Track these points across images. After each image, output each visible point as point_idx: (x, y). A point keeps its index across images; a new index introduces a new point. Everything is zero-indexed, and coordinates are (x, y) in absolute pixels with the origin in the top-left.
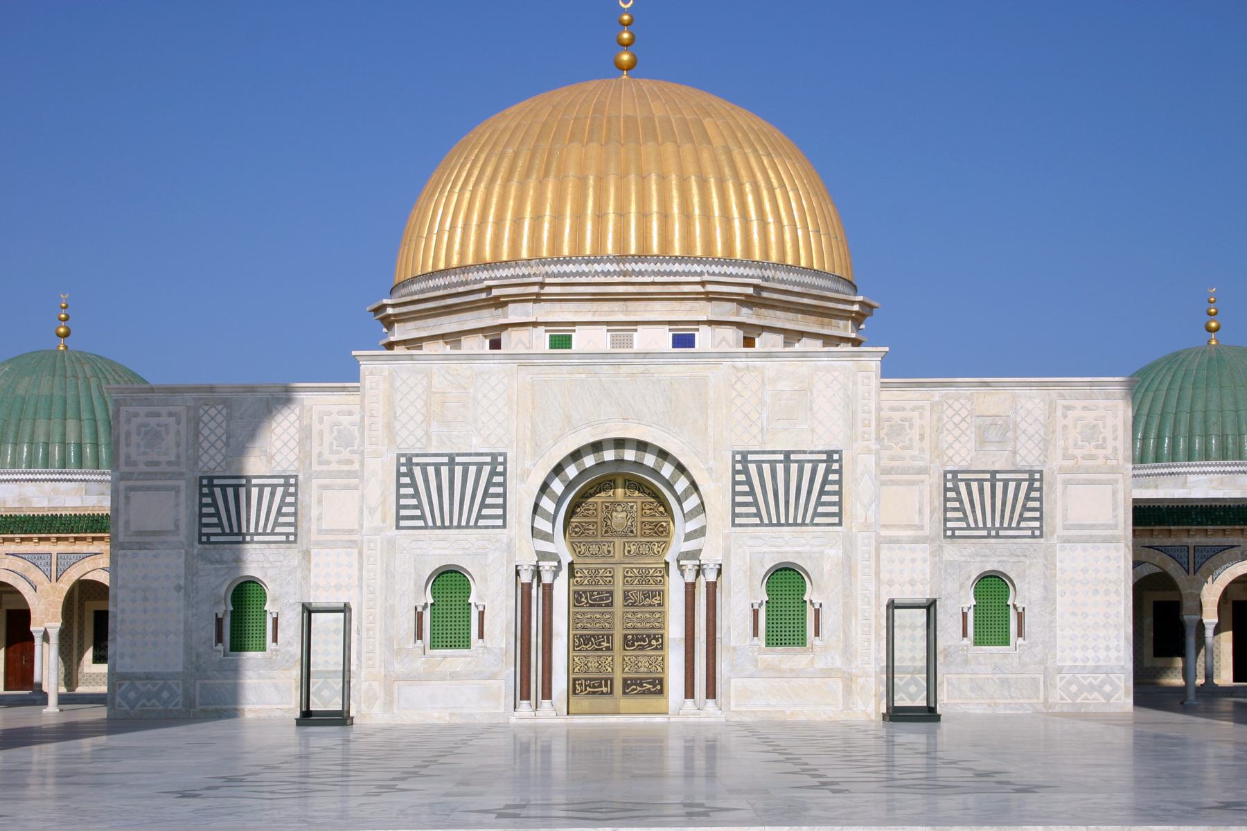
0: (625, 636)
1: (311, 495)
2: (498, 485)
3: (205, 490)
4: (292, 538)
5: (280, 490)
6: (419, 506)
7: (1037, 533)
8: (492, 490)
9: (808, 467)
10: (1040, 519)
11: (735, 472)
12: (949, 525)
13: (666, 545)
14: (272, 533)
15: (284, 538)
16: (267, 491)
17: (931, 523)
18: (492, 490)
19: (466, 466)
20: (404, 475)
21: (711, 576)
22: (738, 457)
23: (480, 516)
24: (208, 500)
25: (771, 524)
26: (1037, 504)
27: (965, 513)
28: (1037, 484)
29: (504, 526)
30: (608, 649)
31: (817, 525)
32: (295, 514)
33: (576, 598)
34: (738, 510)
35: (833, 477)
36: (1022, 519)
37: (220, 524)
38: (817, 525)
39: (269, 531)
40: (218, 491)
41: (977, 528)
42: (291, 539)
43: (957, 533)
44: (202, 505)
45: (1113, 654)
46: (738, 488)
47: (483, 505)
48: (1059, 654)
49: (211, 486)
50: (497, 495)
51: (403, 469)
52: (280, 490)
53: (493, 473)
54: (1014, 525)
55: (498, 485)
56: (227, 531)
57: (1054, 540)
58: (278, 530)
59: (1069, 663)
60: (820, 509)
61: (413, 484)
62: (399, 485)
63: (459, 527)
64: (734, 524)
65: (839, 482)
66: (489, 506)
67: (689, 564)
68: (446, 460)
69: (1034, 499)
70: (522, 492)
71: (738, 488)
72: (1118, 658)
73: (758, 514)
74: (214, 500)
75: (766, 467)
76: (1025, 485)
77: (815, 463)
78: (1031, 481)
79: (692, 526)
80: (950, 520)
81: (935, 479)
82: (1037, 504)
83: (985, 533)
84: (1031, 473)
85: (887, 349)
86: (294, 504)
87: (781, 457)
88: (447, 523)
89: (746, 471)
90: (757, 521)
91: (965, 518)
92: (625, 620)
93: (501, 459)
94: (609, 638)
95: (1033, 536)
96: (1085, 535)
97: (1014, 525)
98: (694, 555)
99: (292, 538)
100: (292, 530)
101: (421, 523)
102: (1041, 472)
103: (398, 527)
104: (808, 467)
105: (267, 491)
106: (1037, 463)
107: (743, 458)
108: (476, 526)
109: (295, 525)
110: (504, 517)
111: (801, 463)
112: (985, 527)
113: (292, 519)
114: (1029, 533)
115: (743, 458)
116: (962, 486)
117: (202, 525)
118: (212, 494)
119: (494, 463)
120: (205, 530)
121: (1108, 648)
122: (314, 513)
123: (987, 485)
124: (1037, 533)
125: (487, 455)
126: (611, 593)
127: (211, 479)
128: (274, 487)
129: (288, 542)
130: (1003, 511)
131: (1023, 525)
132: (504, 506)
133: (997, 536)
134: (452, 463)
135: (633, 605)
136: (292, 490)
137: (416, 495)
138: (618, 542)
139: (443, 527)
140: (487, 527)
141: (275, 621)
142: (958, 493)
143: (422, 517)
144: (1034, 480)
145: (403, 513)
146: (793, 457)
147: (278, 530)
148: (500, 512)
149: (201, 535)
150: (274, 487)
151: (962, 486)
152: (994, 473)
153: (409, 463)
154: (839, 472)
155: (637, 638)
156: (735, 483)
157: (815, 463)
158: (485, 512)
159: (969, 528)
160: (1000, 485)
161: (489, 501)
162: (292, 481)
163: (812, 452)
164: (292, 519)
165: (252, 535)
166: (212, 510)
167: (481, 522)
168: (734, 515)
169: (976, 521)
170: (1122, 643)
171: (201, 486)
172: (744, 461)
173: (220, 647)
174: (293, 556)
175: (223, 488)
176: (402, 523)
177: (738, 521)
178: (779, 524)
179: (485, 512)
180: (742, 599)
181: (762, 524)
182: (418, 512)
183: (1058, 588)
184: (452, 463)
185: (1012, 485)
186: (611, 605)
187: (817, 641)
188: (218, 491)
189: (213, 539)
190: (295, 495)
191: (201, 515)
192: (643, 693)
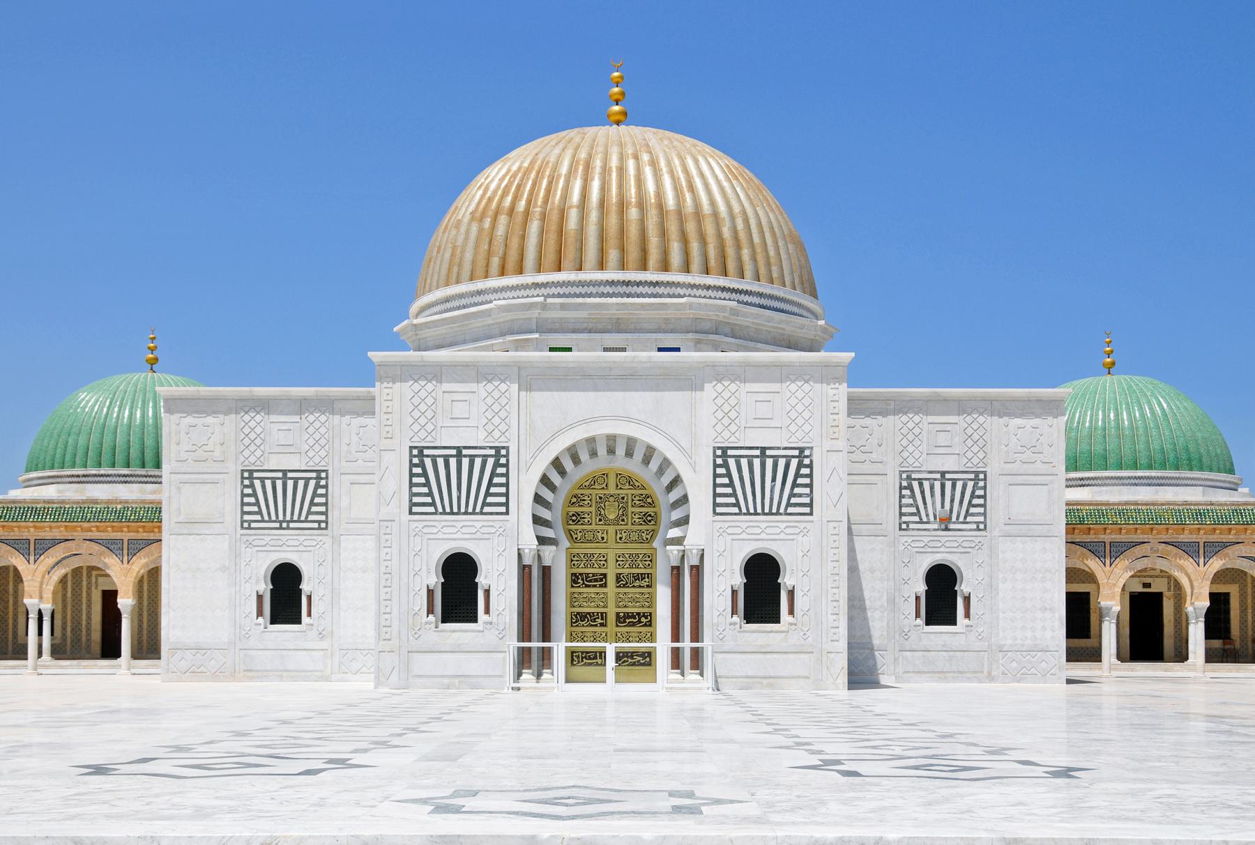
0: (618, 614)
1: (338, 488)
2: (502, 475)
3: (247, 482)
4: (323, 525)
5: (312, 483)
6: (430, 494)
7: (982, 526)
8: (496, 480)
9: (782, 462)
10: (985, 514)
11: (716, 466)
12: (904, 519)
13: (654, 533)
14: (306, 521)
15: (316, 525)
16: (301, 484)
17: (890, 516)
18: (496, 480)
19: (472, 459)
20: (416, 465)
21: (695, 562)
22: (719, 452)
23: (484, 504)
24: (249, 491)
25: (748, 513)
26: (981, 501)
27: (918, 509)
28: (981, 484)
29: (507, 513)
30: (602, 625)
31: (790, 514)
32: (326, 504)
33: (575, 579)
34: (719, 500)
35: (805, 471)
37: (260, 513)
38: (790, 514)
39: (303, 518)
40: (257, 483)
42: (323, 526)
44: (243, 495)
45: (1048, 634)
46: (719, 481)
47: (488, 494)
48: (1001, 634)
49: (251, 478)
50: (501, 485)
51: (416, 461)
52: (312, 483)
53: (497, 465)
54: (961, 519)
55: (502, 475)
56: (266, 518)
57: (996, 533)
58: (311, 518)
59: (1009, 642)
60: (793, 500)
61: (425, 474)
62: (412, 475)
63: (466, 513)
64: (715, 513)
65: (810, 476)
66: (494, 496)
67: (674, 550)
68: (454, 452)
69: (979, 497)
70: (524, 485)
71: (719, 481)
72: (1052, 637)
73: (737, 505)
74: (254, 491)
75: (744, 462)
76: (970, 484)
77: (789, 459)
78: (976, 479)
79: (676, 515)
80: (905, 514)
81: (893, 481)
82: (981, 501)
84: (977, 473)
85: (853, 354)
86: (326, 495)
87: (757, 452)
88: (455, 510)
89: (725, 465)
90: (736, 510)
92: (618, 599)
93: (503, 452)
94: (603, 616)
95: (978, 529)
96: (1023, 529)
97: (961, 519)
98: (678, 541)
99: (323, 525)
100: (323, 518)
101: (432, 509)
102: (985, 473)
103: (411, 513)
104: (782, 462)
105: (301, 484)
106: (981, 464)
107: (723, 453)
108: (482, 513)
109: (325, 513)
110: (506, 504)
111: (776, 458)
113: (323, 509)
114: (974, 526)
115: (723, 453)
116: (915, 485)
117: (243, 513)
118: (252, 486)
119: (498, 456)
120: (246, 517)
121: (1044, 628)
122: (344, 503)
124: (982, 526)
125: (491, 448)
126: (605, 575)
127: (251, 472)
128: (307, 480)
129: (320, 528)
132: (507, 495)
134: (459, 456)
135: (624, 586)
136: (323, 482)
137: (427, 484)
138: (611, 529)
139: (452, 513)
140: (491, 514)
141: (309, 598)
142: (912, 491)
143: (433, 504)
144: (979, 477)
145: (416, 500)
146: (768, 452)
147: (311, 518)
148: (503, 500)
149: (243, 521)
150: (307, 480)
152: (943, 474)
153: (421, 455)
154: (810, 466)
155: (627, 616)
156: (716, 476)
157: (789, 459)
158: (490, 500)
159: (921, 522)
160: (948, 485)
161: (493, 490)
162: (323, 475)
163: (786, 448)
164: (323, 509)
165: (288, 522)
166: (252, 500)
167: (486, 509)
168: (715, 505)
170: (1057, 624)
171: (243, 478)
172: (724, 455)
173: (260, 619)
174: (324, 539)
175: (262, 480)
176: (415, 509)
177: (719, 510)
178: (756, 514)
179: (490, 500)
180: (724, 581)
181: (740, 514)
182: (429, 500)
183: (1001, 576)
184: (459, 456)
185: (959, 485)
186: (605, 585)
187: (790, 619)
188: (257, 483)
189: (253, 525)
190: (326, 487)
191: (243, 504)
192: (634, 664)
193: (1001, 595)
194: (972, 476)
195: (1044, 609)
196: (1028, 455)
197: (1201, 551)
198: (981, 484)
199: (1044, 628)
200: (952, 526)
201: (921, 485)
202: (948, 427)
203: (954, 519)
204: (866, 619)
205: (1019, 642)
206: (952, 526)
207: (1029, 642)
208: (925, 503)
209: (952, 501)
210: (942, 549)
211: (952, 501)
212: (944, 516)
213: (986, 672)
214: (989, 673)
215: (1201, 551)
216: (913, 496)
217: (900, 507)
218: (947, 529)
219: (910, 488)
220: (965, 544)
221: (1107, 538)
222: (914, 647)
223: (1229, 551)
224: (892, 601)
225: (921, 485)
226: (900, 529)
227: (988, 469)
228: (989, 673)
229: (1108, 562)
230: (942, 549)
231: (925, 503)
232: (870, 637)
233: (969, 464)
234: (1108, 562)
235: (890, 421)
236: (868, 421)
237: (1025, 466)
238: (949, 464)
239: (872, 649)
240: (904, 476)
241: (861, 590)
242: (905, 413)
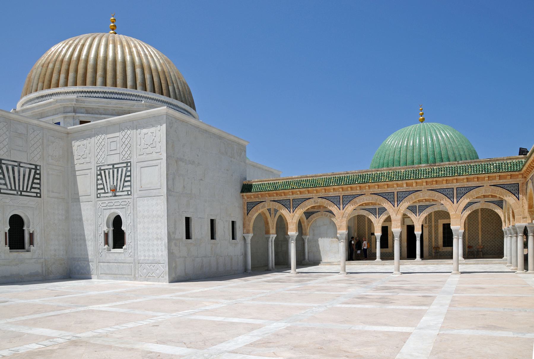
7: (129, 193)
28: (129, 169)
36: (124, 186)
41: (107, 193)
43: (102, 195)
45: (160, 253)
48: (139, 253)
59: (143, 258)
69: (128, 176)
72: (162, 255)
76: (125, 169)
81: (94, 172)
83: (15, 192)
84: (127, 163)
91: (103, 189)
96: (148, 193)
112: (15, 190)
114: (126, 193)
116: (103, 172)
123: (111, 171)
130: (19, 180)
131: (125, 189)
133: (21, 195)
142: (102, 176)
151: (103, 172)
152: (113, 165)
159: (105, 193)
160: (116, 170)
163: (9, 160)
169: (11, 186)
170: (163, 247)
185: (120, 170)
193: (138, 231)
194: (125, 165)
195: (158, 239)
196: (150, 150)
197: (341, 201)
198: (129, 169)
199: (158, 250)
200: (117, 194)
201: (105, 172)
202: (115, 139)
203: (118, 190)
204: (86, 245)
205: (147, 258)
206: (117, 194)
207: (151, 258)
208: (106, 182)
209: (117, 180)
210: (114, 207)
211: (117, 180)
212: (113, 188)
213: (133, 274)
214: (135, 275)
215: (341, 201)
216: (102, 179)
217: (97, 185)
218: (115, 196)
219: (101, 175)
220: (123, 203)
221: (291, 197)
222: (104, 261)
223: (357, 200)
224: (95, 236)
225: (105, 172)
226: (97, 197)
227: (131, 160)
228: (135, 275)
229: (292, 210)
230: (114, 207)
231: (106, 182)
232: (88, 255)
233: (124, 159)
234: (292, 210)
235: (94, 140)
236: (85, 142)
237: (148, 156)
238: (115, 159)
239: (88, 261)
240: (98, 169)
241: (84, 230)
242: (98, 135)
